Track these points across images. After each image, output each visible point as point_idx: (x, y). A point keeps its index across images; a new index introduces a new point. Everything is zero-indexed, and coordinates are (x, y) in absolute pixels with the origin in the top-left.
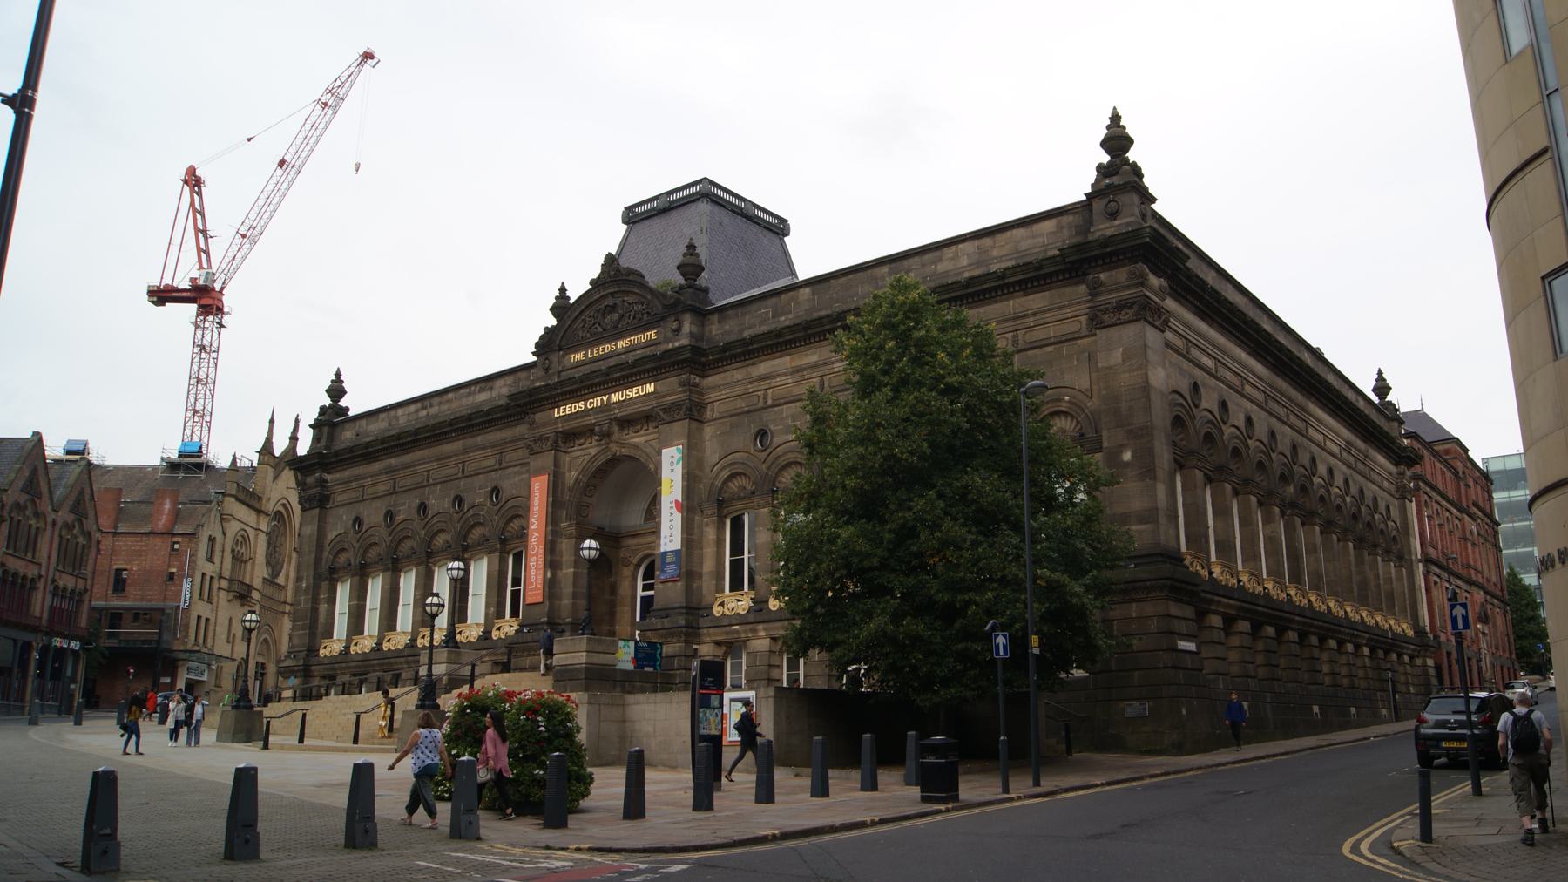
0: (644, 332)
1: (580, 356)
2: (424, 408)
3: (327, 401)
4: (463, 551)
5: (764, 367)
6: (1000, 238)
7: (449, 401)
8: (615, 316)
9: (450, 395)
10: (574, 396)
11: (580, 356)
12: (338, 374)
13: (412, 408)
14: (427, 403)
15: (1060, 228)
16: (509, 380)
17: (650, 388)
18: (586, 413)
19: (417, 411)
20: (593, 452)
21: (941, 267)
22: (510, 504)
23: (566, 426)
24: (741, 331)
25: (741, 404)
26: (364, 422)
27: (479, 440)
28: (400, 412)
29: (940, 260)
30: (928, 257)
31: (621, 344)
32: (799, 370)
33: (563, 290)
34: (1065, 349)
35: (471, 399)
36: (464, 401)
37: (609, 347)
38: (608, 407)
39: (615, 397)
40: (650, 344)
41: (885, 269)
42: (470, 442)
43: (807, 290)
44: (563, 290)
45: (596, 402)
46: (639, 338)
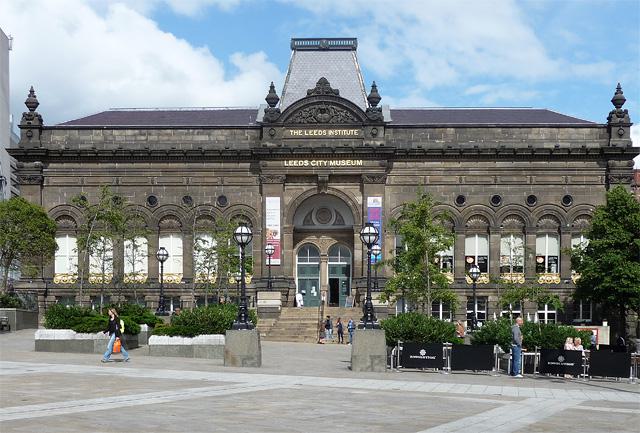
1: (298, 133)
2: (141, 135)
3: (27, 111)
4: (156, 229)
5: (428, 164)
6: (561, 129)
7: (167, 134)
8: (326, 115)
9: (169, 131)
12: (32, 91)
13: (129, 132)
15: (592, 134)
17: (360, 163)
18: (310, 167)
19: (135, 135)
20: (305, 189)
21: (530, 136)
22: (234, 208)
23: (293, 172)
24: (410, 142)
25: (410, 180)
27: (205, 165)
28: (115, 132)
29: (530, 133)
30: (522, 129)
31: (331, 132)
32: (450, 170)
33: (272, 87)
34: (591, 187)
35: (189, 138)
36: (183, 137)
38: (328, 168)
41: (500, 130)
43: (452, 129)
44: (272, 87)
46: (345, 132)
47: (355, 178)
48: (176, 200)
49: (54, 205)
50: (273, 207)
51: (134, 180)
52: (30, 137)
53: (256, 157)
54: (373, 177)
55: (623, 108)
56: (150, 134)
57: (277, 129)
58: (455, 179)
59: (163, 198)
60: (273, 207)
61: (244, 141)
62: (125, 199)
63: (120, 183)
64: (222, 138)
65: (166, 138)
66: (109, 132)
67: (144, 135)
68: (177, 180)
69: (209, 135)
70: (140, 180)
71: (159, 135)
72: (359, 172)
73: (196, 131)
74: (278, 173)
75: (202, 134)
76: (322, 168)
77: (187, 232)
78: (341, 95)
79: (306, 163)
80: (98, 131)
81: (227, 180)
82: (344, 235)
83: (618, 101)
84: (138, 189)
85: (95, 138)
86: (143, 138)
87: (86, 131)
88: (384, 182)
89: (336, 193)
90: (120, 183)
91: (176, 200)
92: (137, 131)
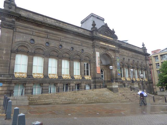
0: (111, 38)
1: (101, 35)
2: (57, 23)
7: (66, 25)
9: (66, 25)
10: (104, 42)
11: (101, 35)
13: (53, 21)
14: (58, 22)
16: (83, 30)
17: (115, 47)
18: (105, 45)
26: (32, 14)
27: (78, 38)
28: (48, 19)
31: (108, 37)
35: (73, 29)
37: (106, 37)
38: (109, 46)
39: (110, 45)
40: (111, 40)
42: (75, 37)
45: (107, 45)
46: (110, 38)
47: (114, 51)
48: (69, 48)
49: (19, 40)
50: (98, 54)
51: (54, 38)
52: (10, 8)
53: (93, 38)
54: (117, 51)
55: (145, 46)
56: (60, 23)
57: (98, 33)
58: (127, 55)
59: (65, 46)
60: (98, 54)
61: (88, 34)
62: (51, 44)
63: (49, 37)
64: (82, 31)
65: (65, 26)
66: (45, 18)
67: (58, 23)
68: (69, 41)
69: (78, 29)
70: (58, 39)
71: (63, 25)
72: (114, 49)
73: (74, 27)
74: (98, 45)
75: (76, 28)
76: (108, 46)
77: (71, 60)
78: (110, 28)
79: (104, 44)
80: (41, 17)
81: (83, 45)
82: (103, 66)
83: (143, 45)
84: (56, 42)
85: (40, 18)
86: (58, 24)
87: (36, 15)
88: (119, 53)
89: (109, 54)
90: (49, 37)
91: (69, 48)
92: (56, 21)
